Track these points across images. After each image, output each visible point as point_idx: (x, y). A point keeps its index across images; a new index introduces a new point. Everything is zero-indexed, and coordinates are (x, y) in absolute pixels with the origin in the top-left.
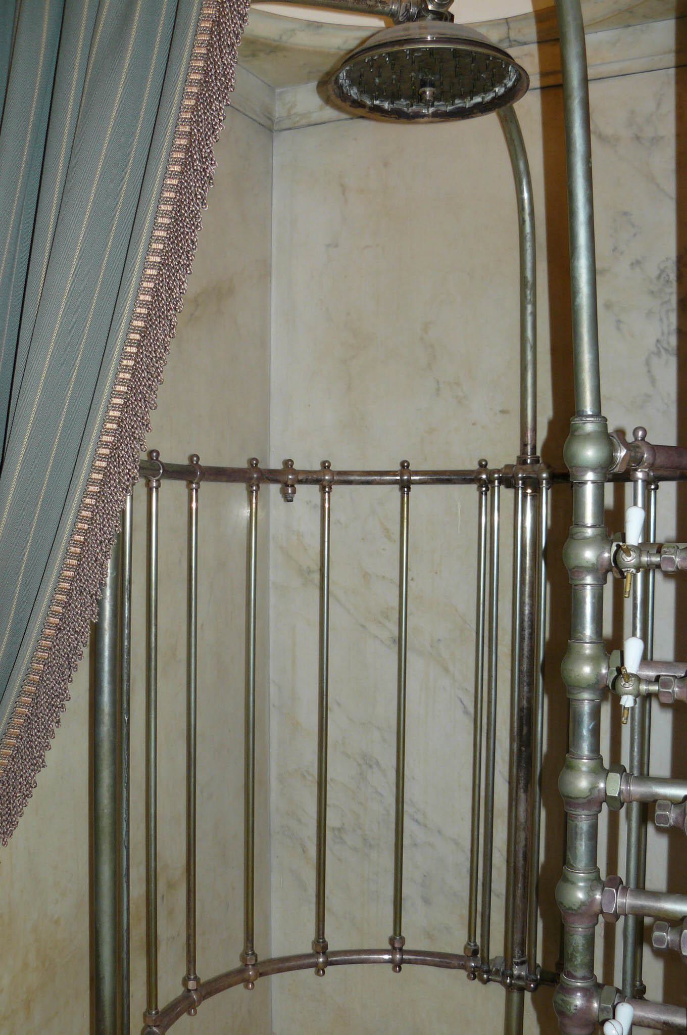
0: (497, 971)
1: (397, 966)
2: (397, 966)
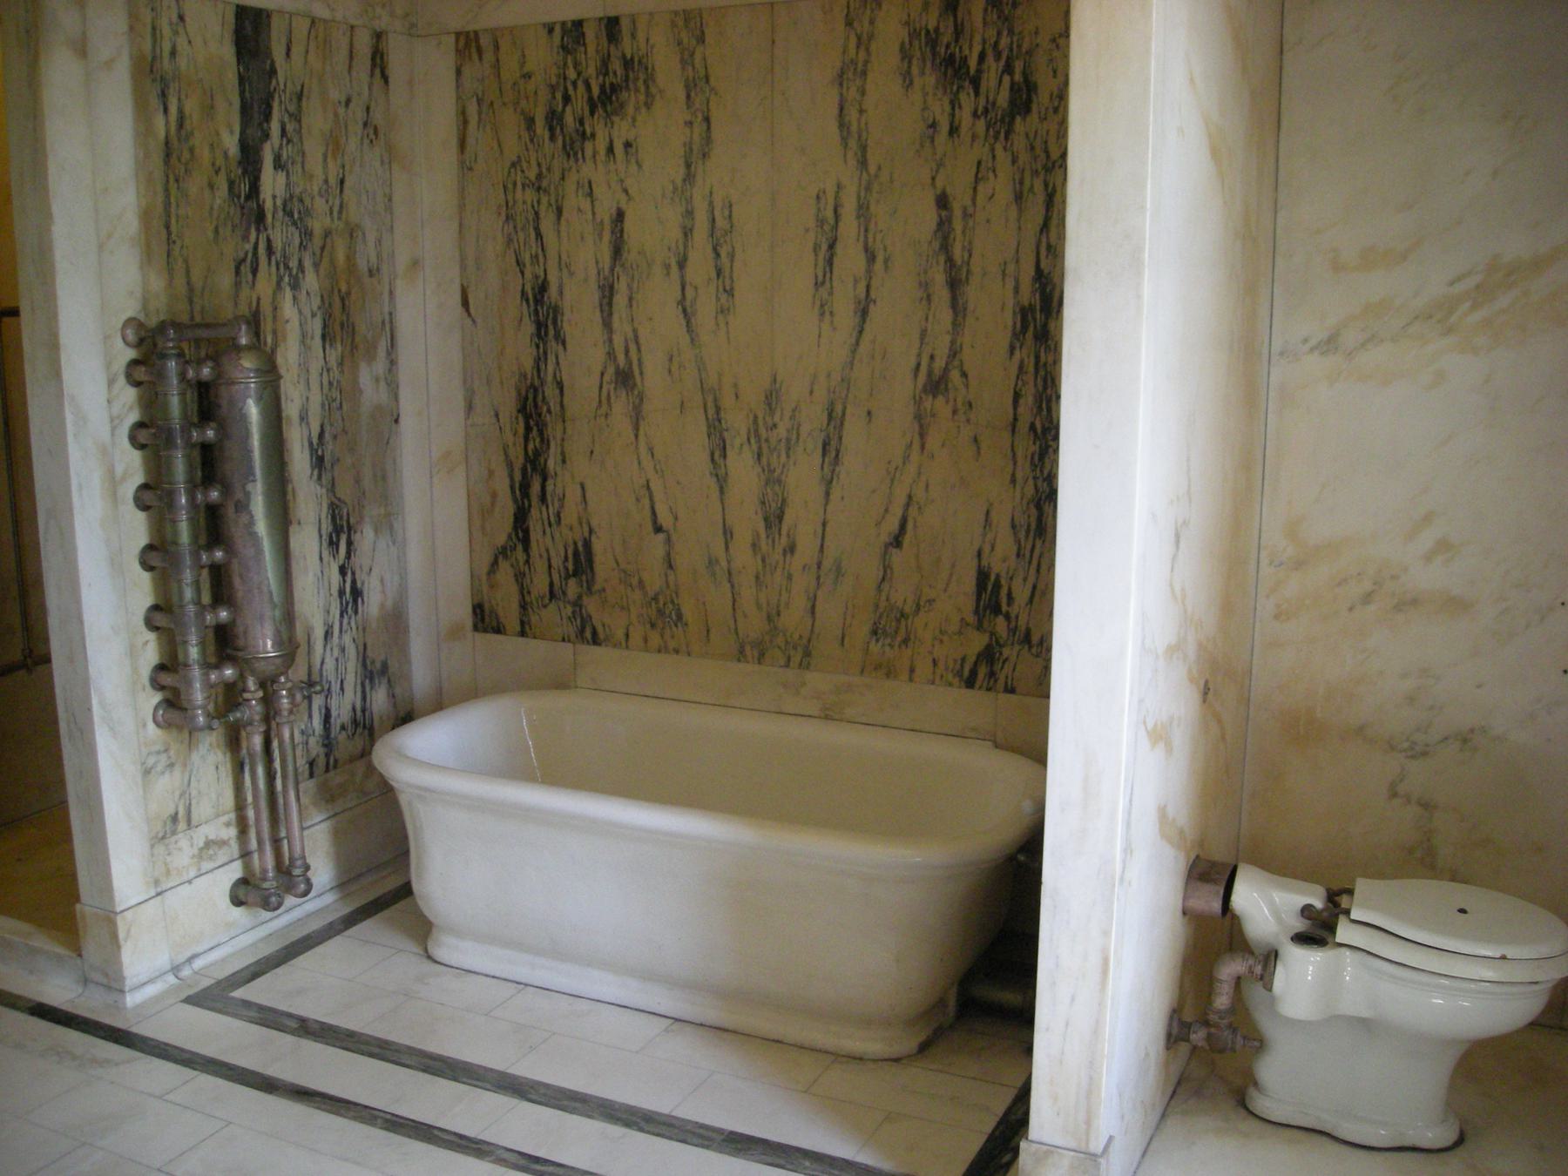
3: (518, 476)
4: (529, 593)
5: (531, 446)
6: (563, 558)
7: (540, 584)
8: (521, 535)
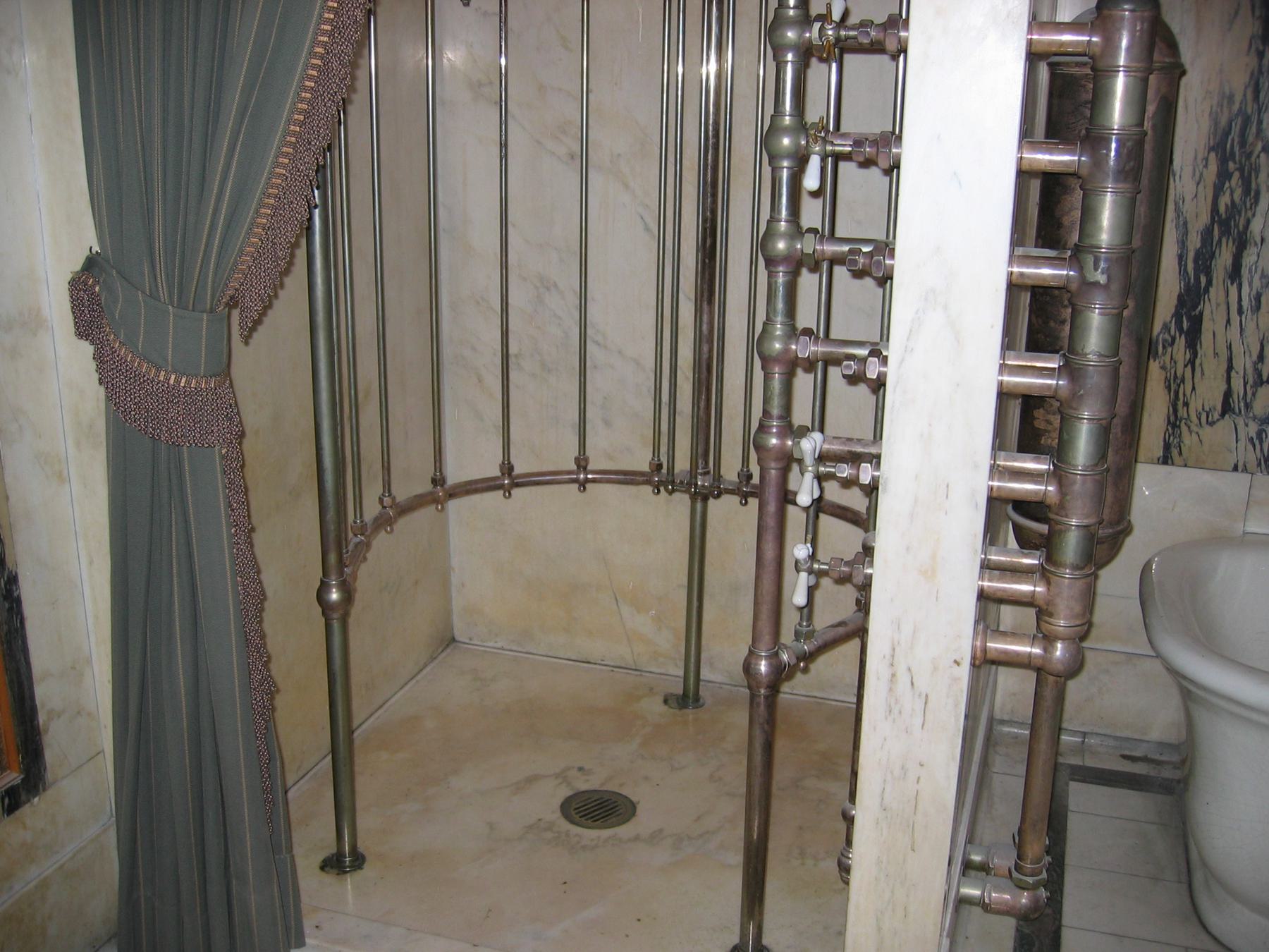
0: (682, 482)
1: (583, 485)
2: (583, 485)
3: (1194, 242)
4: (1186, 404)
5: (1224, 200)
6: (1255, 358)
7: (1208, 391)
8: (1185, 325)
